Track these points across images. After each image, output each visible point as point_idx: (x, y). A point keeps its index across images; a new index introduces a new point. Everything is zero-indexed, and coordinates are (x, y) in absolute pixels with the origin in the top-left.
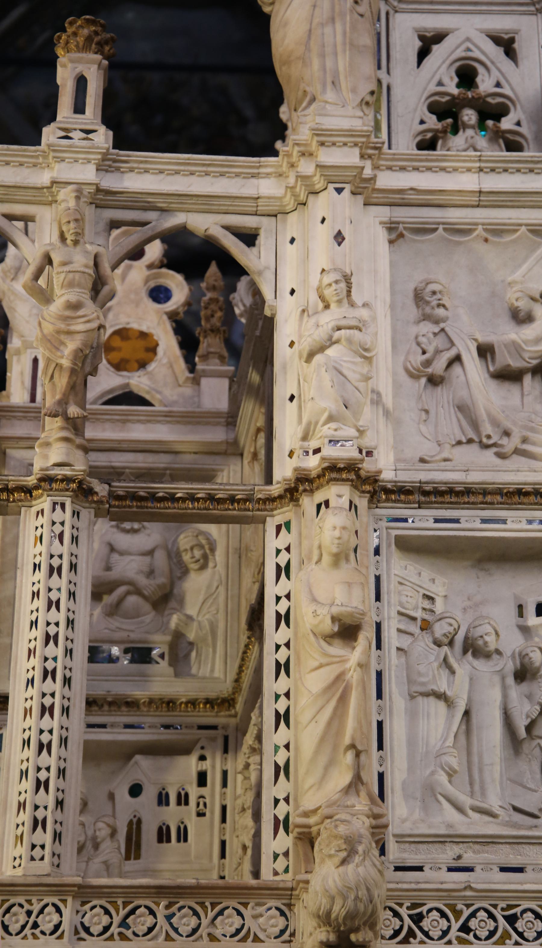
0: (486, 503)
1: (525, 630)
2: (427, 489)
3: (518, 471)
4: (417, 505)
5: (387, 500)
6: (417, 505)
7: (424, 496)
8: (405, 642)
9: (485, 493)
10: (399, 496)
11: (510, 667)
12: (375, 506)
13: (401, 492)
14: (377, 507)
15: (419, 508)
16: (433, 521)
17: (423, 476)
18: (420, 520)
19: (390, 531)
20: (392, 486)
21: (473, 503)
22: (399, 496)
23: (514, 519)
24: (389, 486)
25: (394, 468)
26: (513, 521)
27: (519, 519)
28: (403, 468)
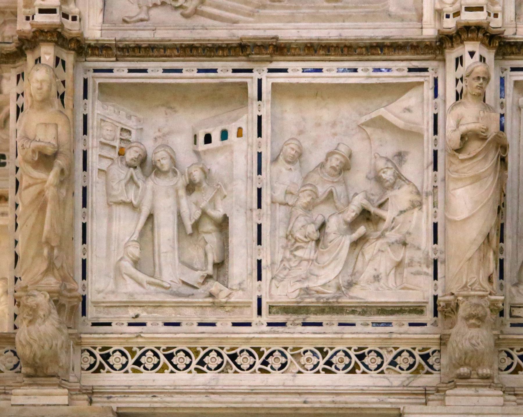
0: (166, 56)
1: (197, 153)
2: (121, 46)
3: (194, 29)
4: (114, 59)
5: (93, 55)
6: (114, 59)
7: (119, 51)
8: (105, 164)
9: (165, 48)
10: (102, 52)
11: (181, 181)
12: (84, 60)
13: (101, 49)
14: (86, 61)
15: (117, 60)
16: (127, 71)
17: (119, 35)
18: (118, 71)
19: (95, 80)
20: (95, 44)
21: (156, 57)
22: (102, 52)
23: (188, 68)
24: (92, 43)
25: (100, 28)
26: (187, 71)
27: (192, 68)
28: (106, 28)
